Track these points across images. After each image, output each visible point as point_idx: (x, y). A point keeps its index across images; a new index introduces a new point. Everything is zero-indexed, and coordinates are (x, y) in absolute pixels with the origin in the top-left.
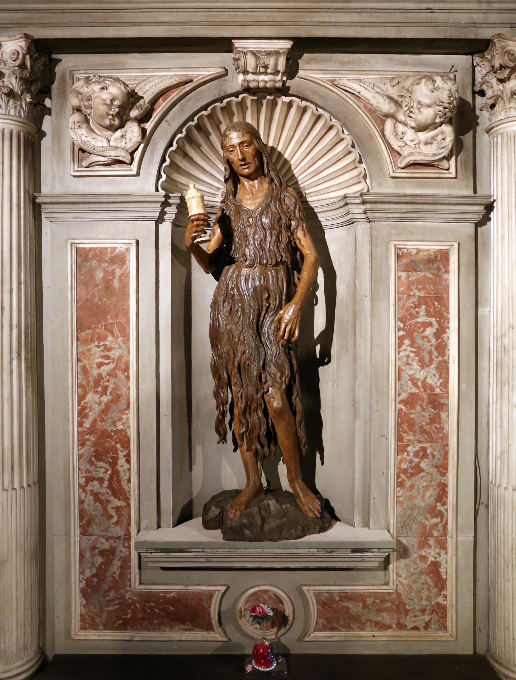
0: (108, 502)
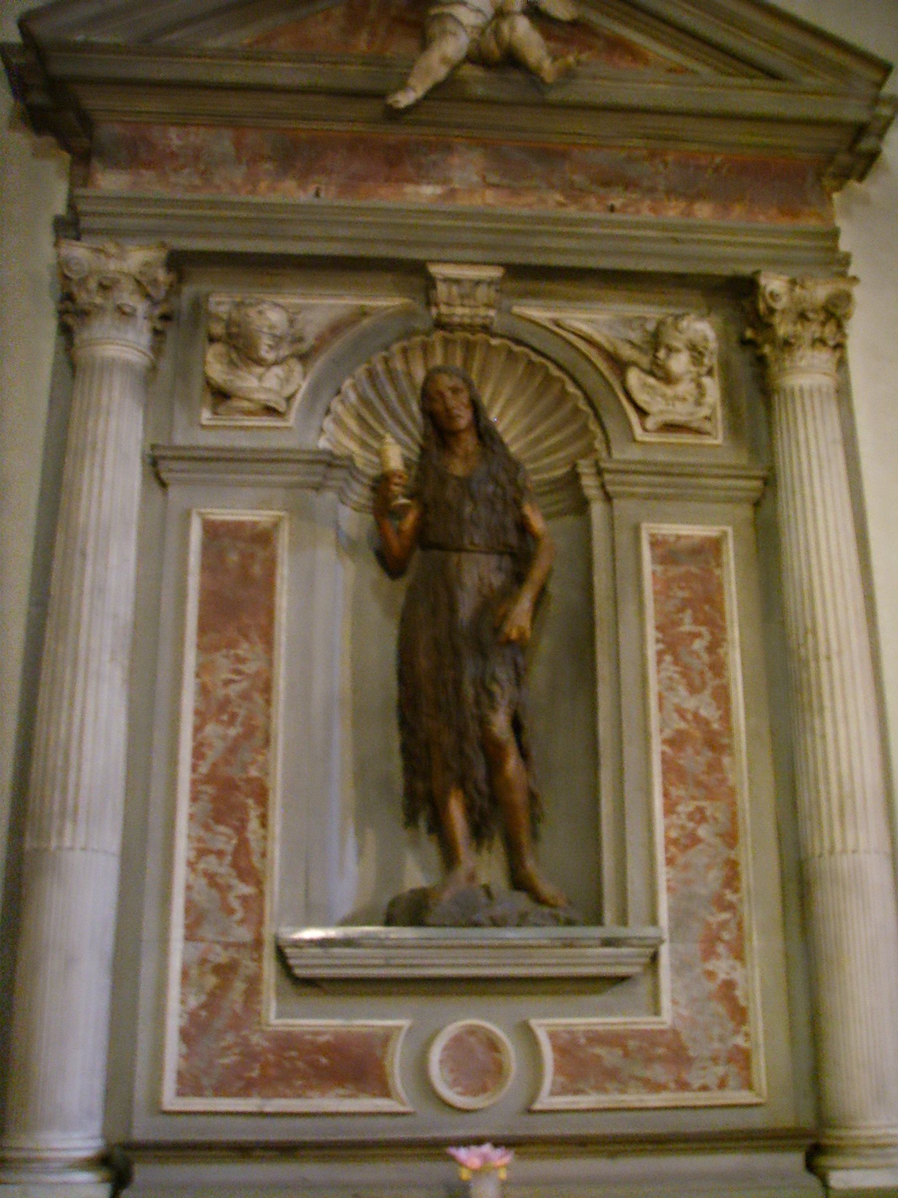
0: (230, 887)
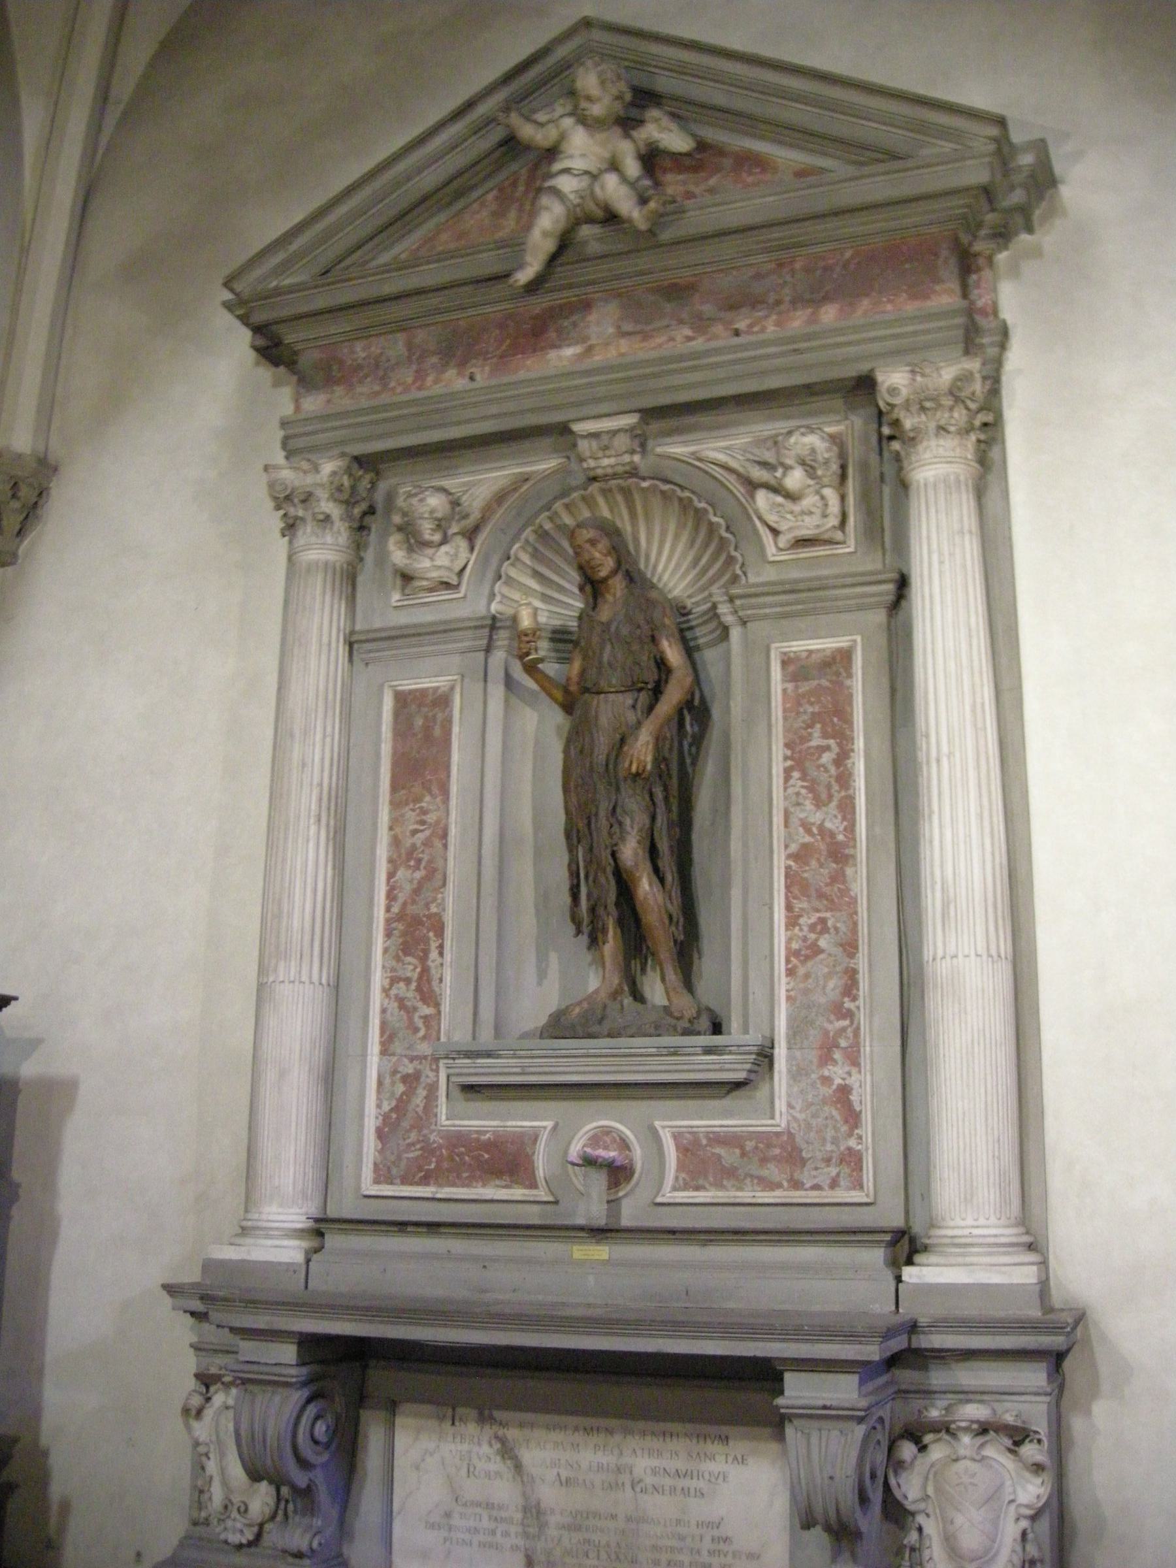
0: (415, 1009)
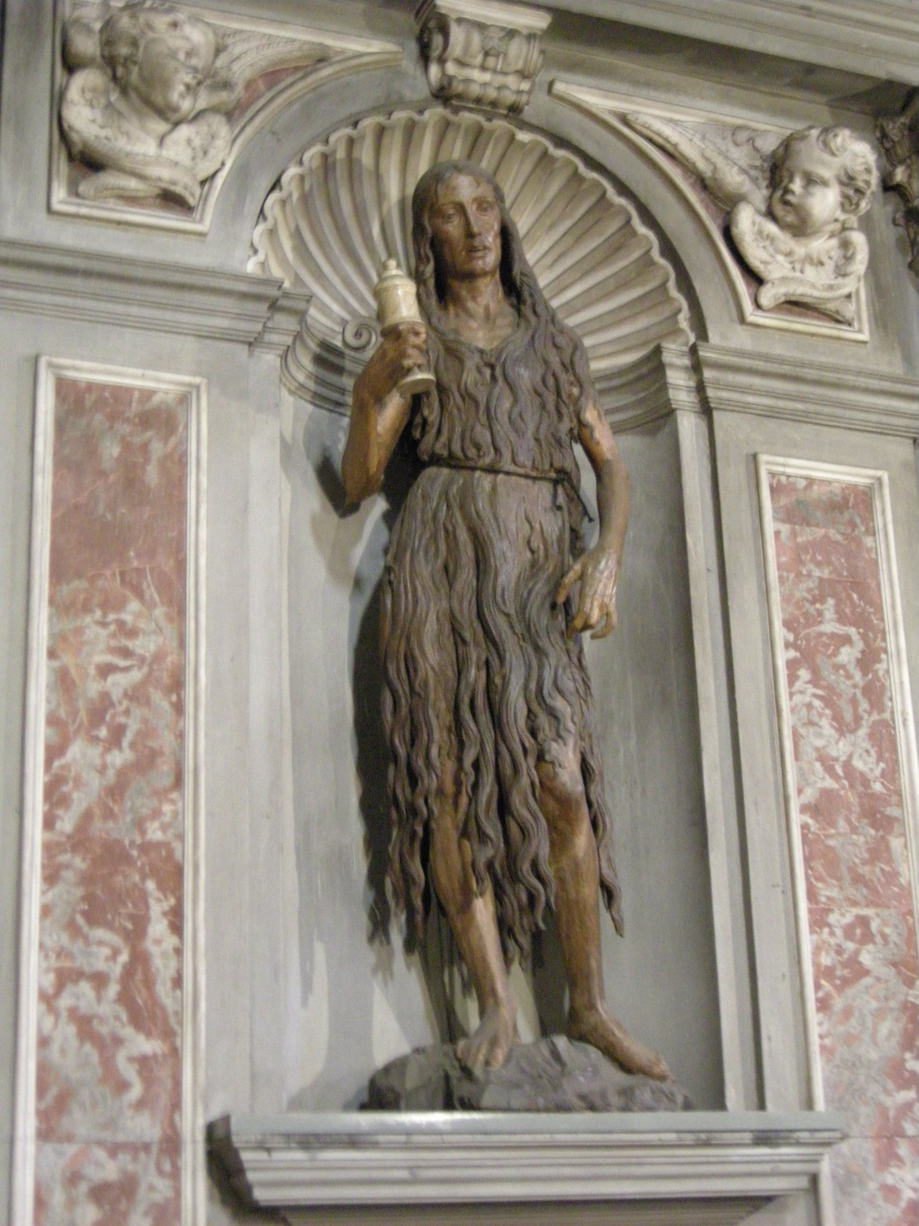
0: (118, 1041)
